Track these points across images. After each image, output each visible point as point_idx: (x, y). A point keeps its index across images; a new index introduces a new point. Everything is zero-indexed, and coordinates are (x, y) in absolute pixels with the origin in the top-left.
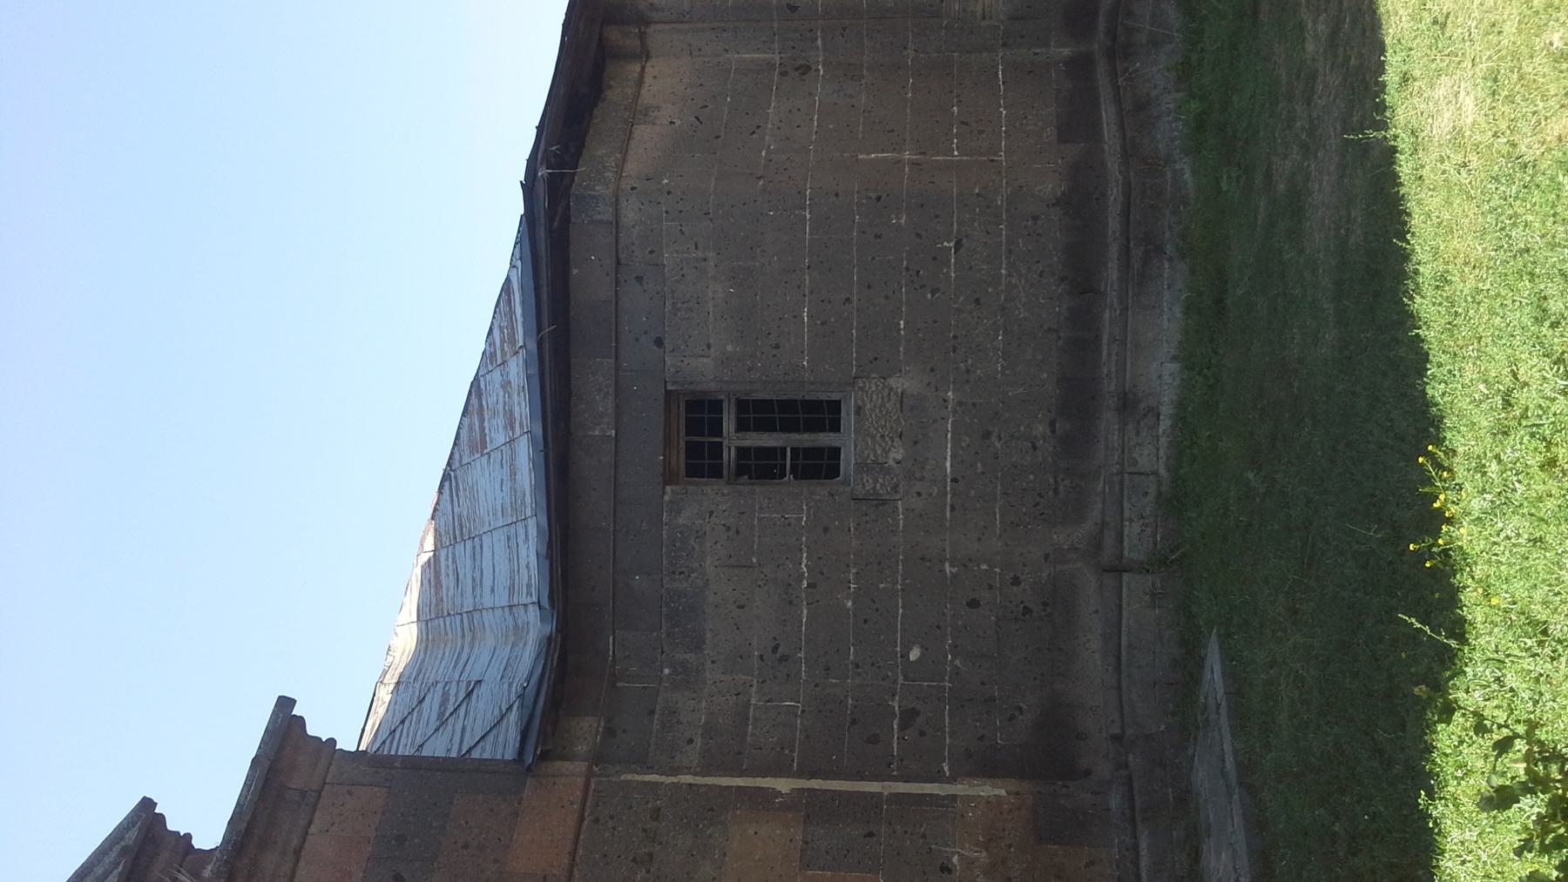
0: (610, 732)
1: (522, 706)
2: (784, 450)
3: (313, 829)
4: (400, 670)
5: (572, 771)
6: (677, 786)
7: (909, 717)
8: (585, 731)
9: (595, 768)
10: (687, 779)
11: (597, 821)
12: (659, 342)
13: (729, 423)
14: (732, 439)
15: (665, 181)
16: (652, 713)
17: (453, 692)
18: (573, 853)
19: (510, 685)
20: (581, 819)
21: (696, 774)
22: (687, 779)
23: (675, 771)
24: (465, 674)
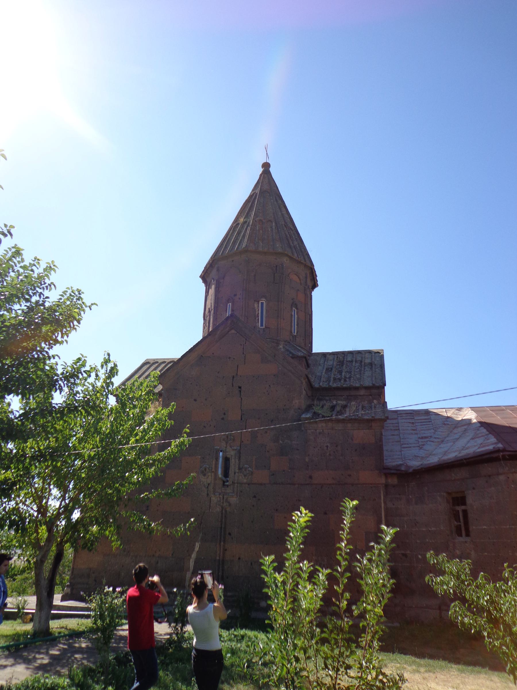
0: (394, 486)
1: (401, 465)
2: (460, 522)
3: (364, 430)
4: (454, 416)
5: (383, 480)
6: (381, 503)
7: (405, 555)
8: (394, 481)
9: (383, 485)
10: (383, 505)
11: (372, 487)
12: (474, 489)
13: (463, 507)
14: (460, 508)
15: (513, 486)
16: (400, 495)
17: (426, 440)
18: (364, 484)
19: (410, 460)
20: (371, 484)
21: (384, 507)
22: (383, 505)
23: (385, 503)
24: (429, 443)
